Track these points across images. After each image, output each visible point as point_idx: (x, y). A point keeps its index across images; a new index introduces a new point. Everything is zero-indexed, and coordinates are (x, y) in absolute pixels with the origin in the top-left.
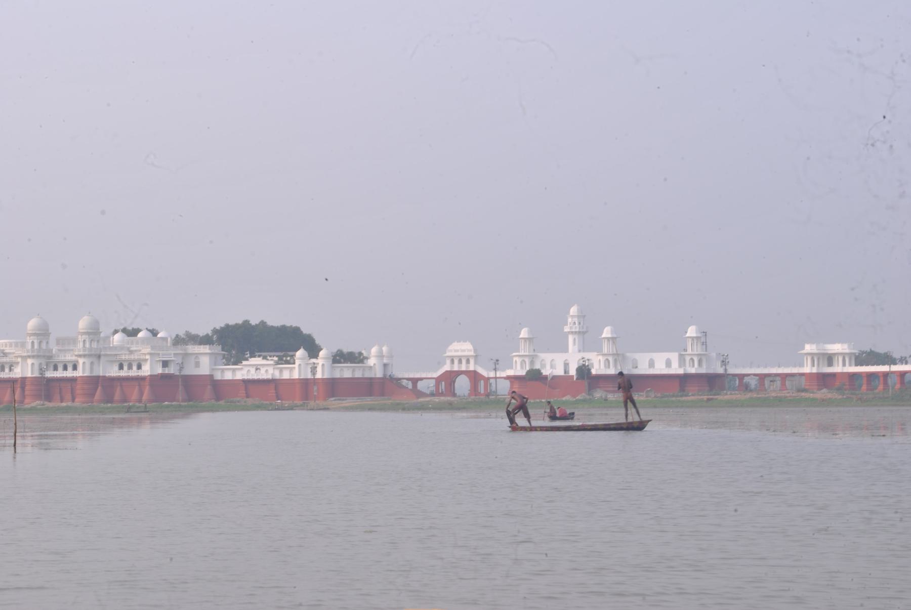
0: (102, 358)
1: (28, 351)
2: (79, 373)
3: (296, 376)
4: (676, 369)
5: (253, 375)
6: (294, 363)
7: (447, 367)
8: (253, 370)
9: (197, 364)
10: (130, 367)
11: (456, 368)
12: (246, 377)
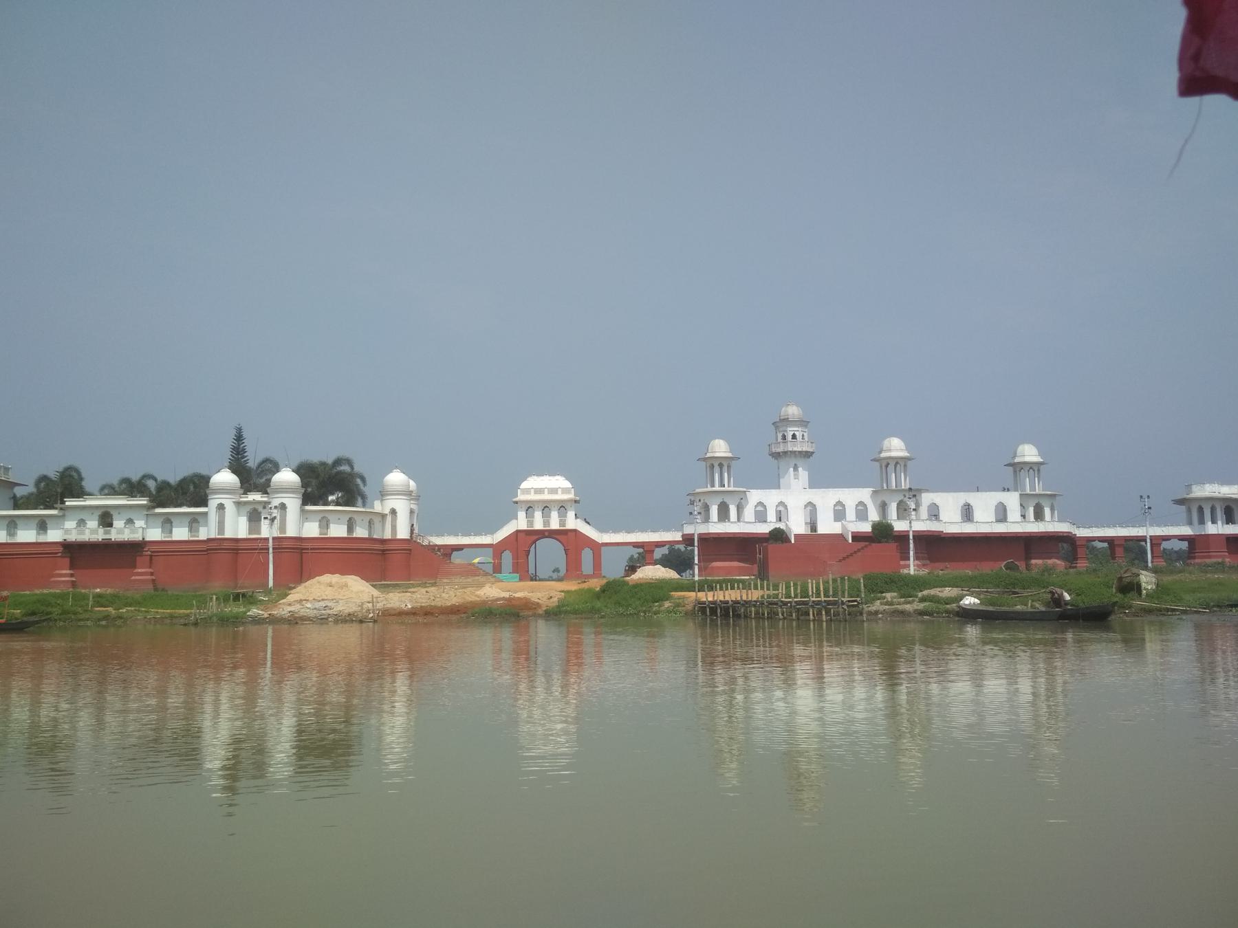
4: (1017, 524)
5: (92, 532)
7: (521, 523)
11: (538, 525)
12: (73, 537)
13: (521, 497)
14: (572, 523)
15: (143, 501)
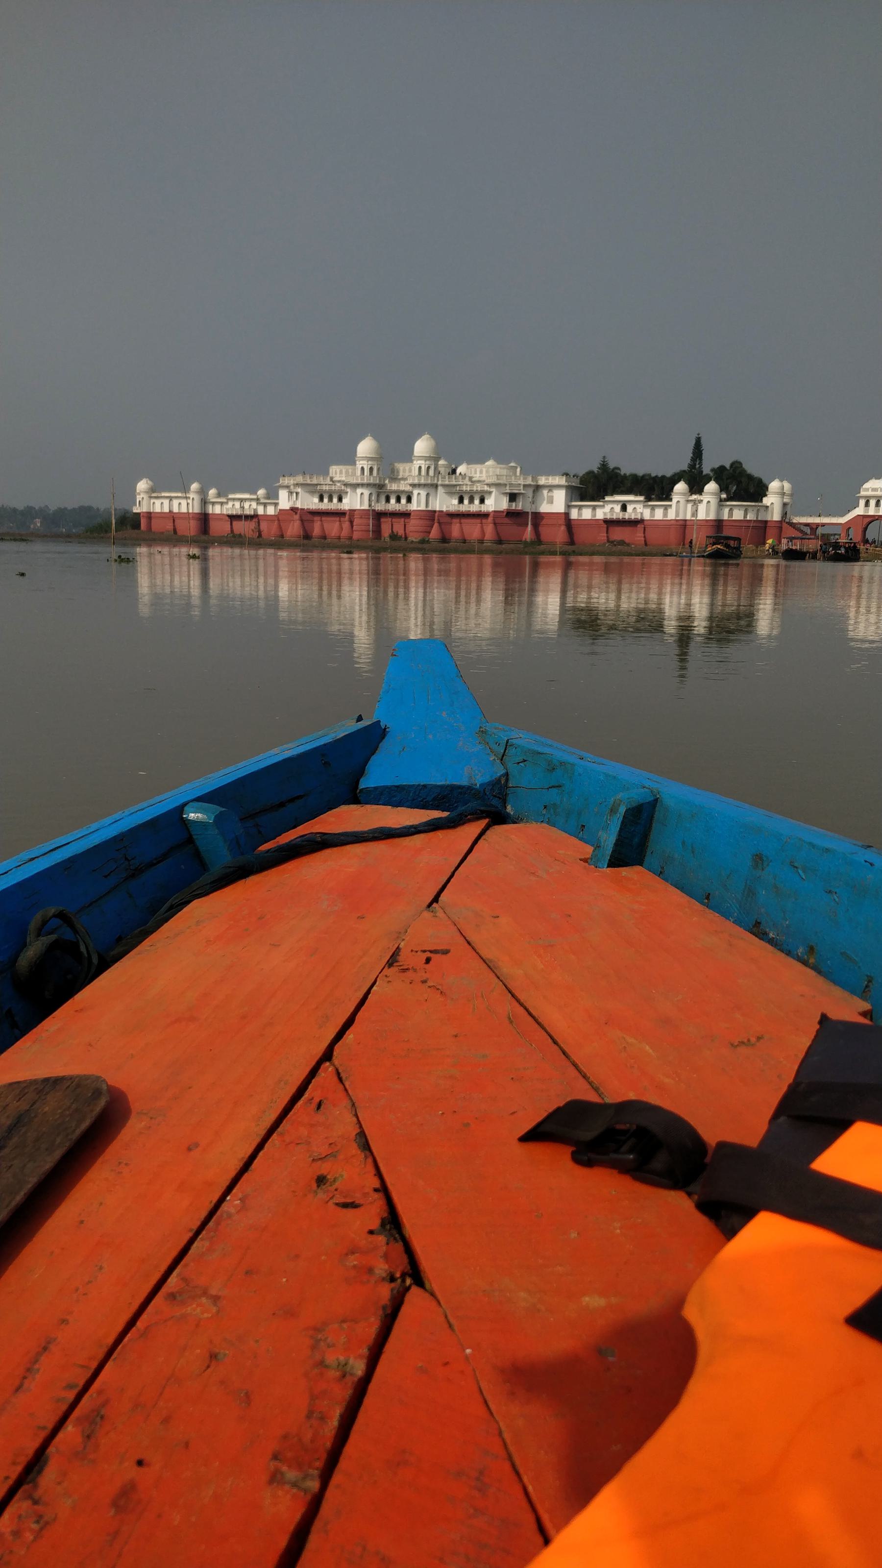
0: (440, 488)
1: (357, 479)
2: (414, 506)
3: (671, 515)
6: (671, 500)
7: (860, 511)
8: (618, 508)
9: (551, 501)
10: (471, 500)
13: (863, 493)
15: (642, 498)
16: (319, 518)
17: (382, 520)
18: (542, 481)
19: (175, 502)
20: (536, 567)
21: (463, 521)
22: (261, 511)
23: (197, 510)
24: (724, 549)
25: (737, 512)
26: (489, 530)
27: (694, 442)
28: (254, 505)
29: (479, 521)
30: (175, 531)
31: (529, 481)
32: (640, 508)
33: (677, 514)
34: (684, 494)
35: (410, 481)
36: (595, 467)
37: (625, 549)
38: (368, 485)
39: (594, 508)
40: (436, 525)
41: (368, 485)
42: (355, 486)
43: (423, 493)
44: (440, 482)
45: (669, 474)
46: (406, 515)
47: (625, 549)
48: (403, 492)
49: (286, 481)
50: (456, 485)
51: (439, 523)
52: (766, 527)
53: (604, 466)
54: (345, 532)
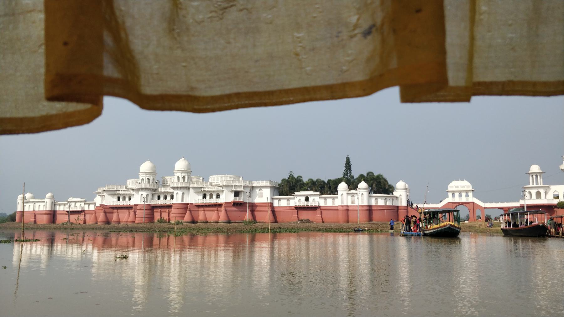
0: (191, 189)
3: (338, 203)
5: (303, 203)
7: (450, 199)
8: (303, 199)
11: (457, 200)
12: (298, 204)
13: (450, 189)
14: (471, 199)
15: (318, 193)
16: (116, 211)
17: (155, 210)
18: (255, 184)
19: (37, 204)
20: (253, 240)
21: (206, 209)
22: (86, 208)
23: (48, 208)
24: (371, 222)
25: (380, 201)
26: (222, 214)
27: (346, 160)
28: (83, 204)
29: (216, 209)
30: (35, 222)
31: (248, 184)
32: (317, 198)
33: (342, 202)
34: (345, 189)
35: (172, 186)
36: (286, 177)
37: (307, 224)
38: (146, 189)
39: (288, 199)
40: (188, 212)
41: (146, 189)
42: (139, 190)
43: (180, 193)
44: (191, 186)
45: (333, 178)
46: (169, 207)
47: (307, 224)
48: (168, 193)
49: (100, 190)
50: (202, 188)
51: (190, 211)
52: (398, 210)
53: (291, 176)
54: (131, 219)
